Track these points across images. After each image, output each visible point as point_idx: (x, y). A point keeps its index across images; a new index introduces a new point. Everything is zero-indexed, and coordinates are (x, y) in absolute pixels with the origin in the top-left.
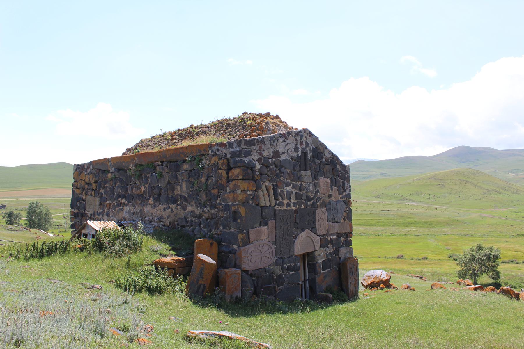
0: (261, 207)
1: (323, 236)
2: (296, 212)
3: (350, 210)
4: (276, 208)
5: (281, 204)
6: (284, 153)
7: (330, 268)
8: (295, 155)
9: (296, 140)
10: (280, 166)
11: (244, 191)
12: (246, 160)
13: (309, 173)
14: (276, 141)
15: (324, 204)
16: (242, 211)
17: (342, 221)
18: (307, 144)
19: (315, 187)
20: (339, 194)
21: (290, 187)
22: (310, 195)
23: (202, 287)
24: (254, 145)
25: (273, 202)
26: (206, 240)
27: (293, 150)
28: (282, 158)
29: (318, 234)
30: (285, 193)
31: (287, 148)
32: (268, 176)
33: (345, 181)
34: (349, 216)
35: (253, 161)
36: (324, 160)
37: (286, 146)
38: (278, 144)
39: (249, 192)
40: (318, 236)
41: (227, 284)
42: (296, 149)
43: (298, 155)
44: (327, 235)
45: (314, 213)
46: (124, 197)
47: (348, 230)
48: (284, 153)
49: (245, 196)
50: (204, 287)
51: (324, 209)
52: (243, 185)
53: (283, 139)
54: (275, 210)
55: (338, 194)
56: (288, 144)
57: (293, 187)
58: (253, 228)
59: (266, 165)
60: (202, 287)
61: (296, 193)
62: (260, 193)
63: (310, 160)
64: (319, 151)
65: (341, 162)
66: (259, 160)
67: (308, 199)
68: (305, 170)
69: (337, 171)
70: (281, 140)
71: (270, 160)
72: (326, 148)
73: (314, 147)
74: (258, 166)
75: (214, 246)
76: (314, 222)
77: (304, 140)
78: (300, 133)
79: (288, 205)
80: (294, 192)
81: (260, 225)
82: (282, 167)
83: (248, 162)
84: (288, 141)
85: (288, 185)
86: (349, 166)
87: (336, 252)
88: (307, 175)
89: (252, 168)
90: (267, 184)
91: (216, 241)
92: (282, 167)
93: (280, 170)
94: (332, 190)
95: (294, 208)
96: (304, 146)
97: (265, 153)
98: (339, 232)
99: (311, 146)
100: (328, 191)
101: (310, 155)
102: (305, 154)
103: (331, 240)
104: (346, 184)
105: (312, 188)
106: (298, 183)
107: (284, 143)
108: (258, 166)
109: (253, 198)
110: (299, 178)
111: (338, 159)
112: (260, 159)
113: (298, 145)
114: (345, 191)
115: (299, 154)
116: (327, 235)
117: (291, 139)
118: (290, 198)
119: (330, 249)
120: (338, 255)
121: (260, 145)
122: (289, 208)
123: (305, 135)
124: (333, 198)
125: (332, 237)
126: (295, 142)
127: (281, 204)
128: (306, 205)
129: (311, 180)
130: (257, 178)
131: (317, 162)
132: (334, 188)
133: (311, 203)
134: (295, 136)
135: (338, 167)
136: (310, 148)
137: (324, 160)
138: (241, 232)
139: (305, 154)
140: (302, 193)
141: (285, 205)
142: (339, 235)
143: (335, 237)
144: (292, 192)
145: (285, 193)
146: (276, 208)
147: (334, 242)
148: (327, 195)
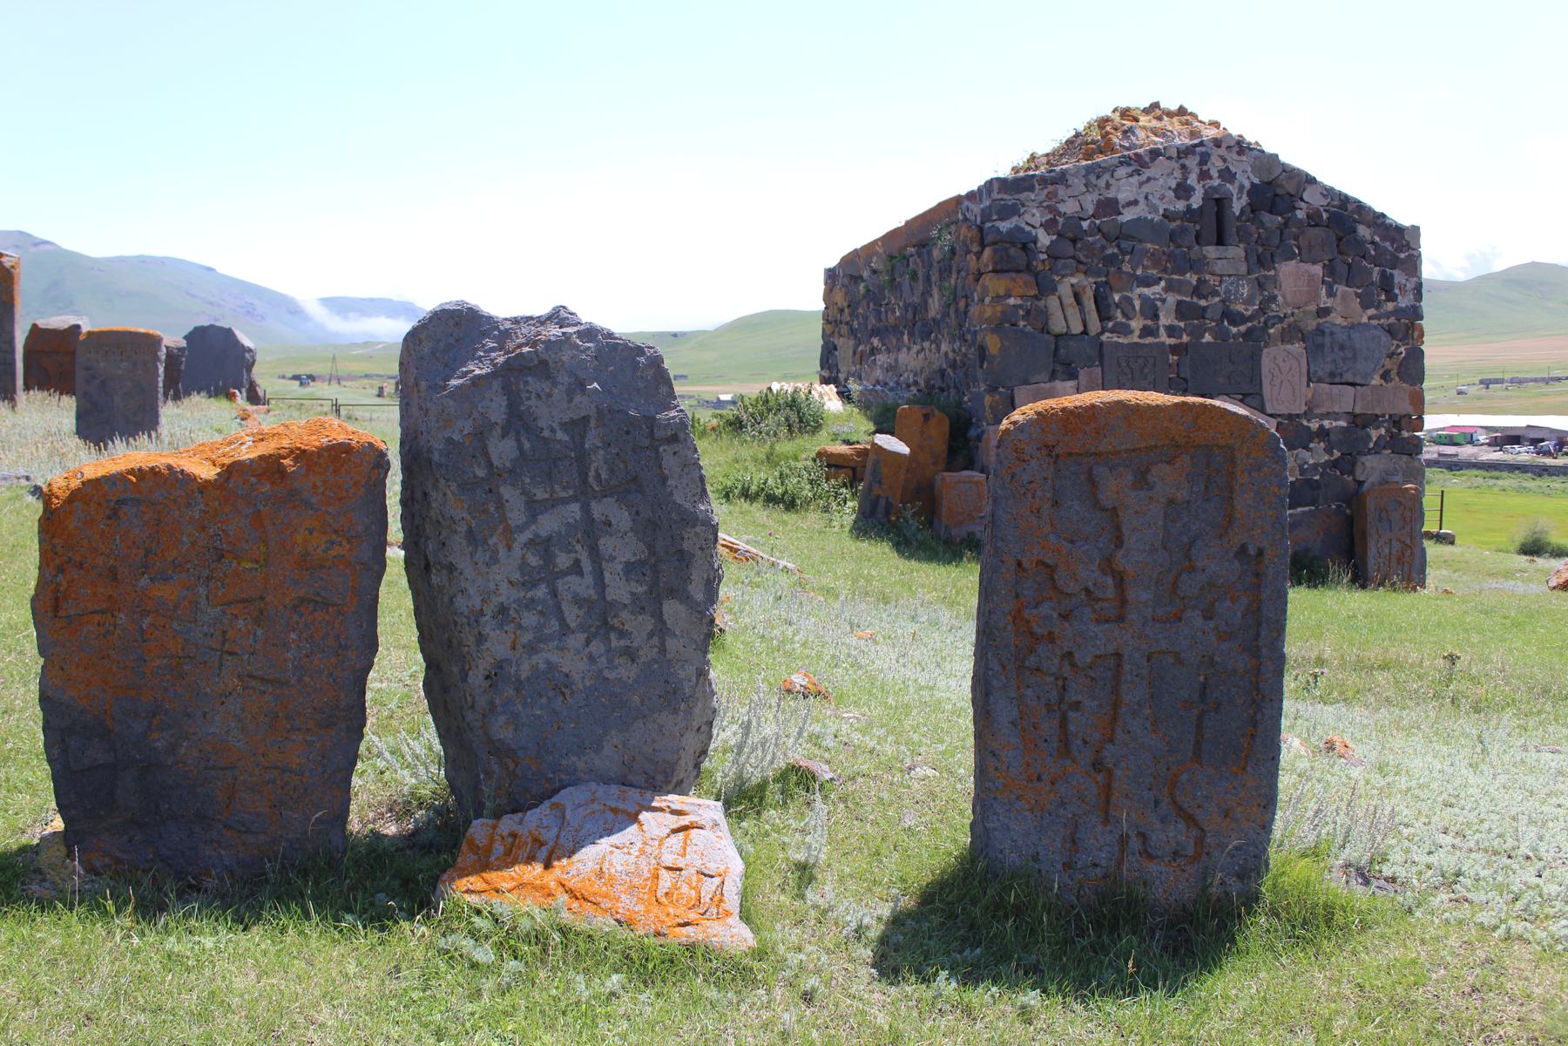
0: (1057, 336)
1: (1290, 417)
2: (1174, 349)
3: (1417, 356)
4: (1104, 338)
5: (1124, 330)
6: (1135, 203)
7: (1314, 502)
8: (1180, 206)
9: (1183, 167)
10: (1121, 235)
11: (998, 298)
12: (1004, 226)
13: (1236, 251)
14: (1107, 176)
15: (1293, 333)
16: (993, 344)
17: (1376, 380)
18: (1227, 175)
19: (1261, 285)
20: (1365, 307)
21: (1157, 289)
22: (1240, 308)
23: (882, 502)
24: (1031, 189)
25: (1094, 325)
26: (916, 407)
27: (1171, 193)
28: (1128, 215)
29: (1269, 411)
30: (1137, 304)
31: (1145, 189)
32: (1080, 262)
33: (1396, 273)
34: (1412, 369)
35: (1028, 228)
36: (1300, 214)
37: (1141, 184)
38: (1112, 181)
39: (1012, 301)
40: (1271, 416)
41: (945, 502)
42: (1183, 191)
43: (1189, 207)
44: (1308, 415)
45: (1255, 359)
46: (875, 332)
47: (1404, 407)
48: (1135, 203)
49: (999, 308)
50: (888, 503)
51: (1298, 348)
52: (994, 284)
53: (1130, 170)
54: (1101, 344)
55: (1359, 309)
56: (1149, 179)
57: (1166, 290)
58: (1026, 382)
59: (1070, 235)
60: (882, 502)
61: (1179, 303)
62: (1052, 302)
63: (1239, 218)
64: (1280, 191)
65: (1383, 216)
66: (1048, 226)
67: (1236, 319)
68: (1220, 241)
69: (1360, 243)
70: (1122, 172)
71: (1085, 225)
72: (1311, 181)
73: (1256, 181)
74: (1044, 239)
75: (933, 422)
76: (1255, 377)
77: (1215, 165)
78: (1198, 149)
79: (1146, 332)
80: (1172, 299)
81: (1053, 378)
82: (1128, 237)
83: (1010, 232)
84: (1147, 173)
85: (1147, 282)
86: (1415, 230)
87: (1346, 463)
88: (1228, 259)
89: (1027, 245)
90: (1074, 280)
91: (942, 410)
92: (1128, 237)
93: (1118, 246)
94: (1331, 294)
95: (1172, 341)
96: (1216, 182)
97: (1069, 207)
98: (1358, 411)
99: (1246, 176)
100: (1317, 297)
101: (1237, 206)
102: (1218, 203)
103: (1323, 433)
104: (1399, 276)
105: (1245, 291)
106: (1192, 278)
107: (1135, 180)
108: (1044, 239)
109: (1028, 312)
110: (1197, 265)
111: (1360, 207)
112: (1053, 222)
113: (1192, 180)
114: (1392, 298)
115: (1196, 201)
116: (1308, 415)
117: (1159, 168)
118: (1156, 317)
119: (1317, 455)
120: (1352, 472)
121: (1050, 188)
122: (1149, 340)
123: (1222, 151)
124: (1336, 319)
125: (1326, 423)
126: (1178, 174)
127: (1127, 331)
128: (1221, 334)
129: (1243, 269)
130: (1040, 267)
131: (1272, 221)
132: (1341, 289)
133: (1243, 328)
134: (1179, 158)
135: (1363, 231)
136: (1242, 187)
137: (1300, 214)
138: (992, 389)
139: (1218, 203)
140: (1203, 303)
141: (1137, 333)
142: (1360, 422)
143: (1343, 424)
144: (1164, 301)
145: (1137, 304)
146: (1104, 338)
147: (1333, 437)
148: (1312, 308)
